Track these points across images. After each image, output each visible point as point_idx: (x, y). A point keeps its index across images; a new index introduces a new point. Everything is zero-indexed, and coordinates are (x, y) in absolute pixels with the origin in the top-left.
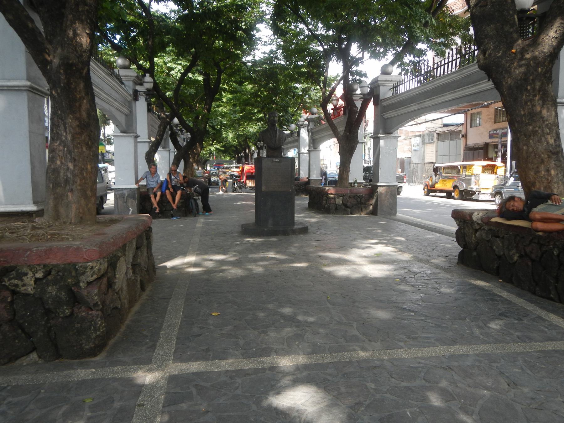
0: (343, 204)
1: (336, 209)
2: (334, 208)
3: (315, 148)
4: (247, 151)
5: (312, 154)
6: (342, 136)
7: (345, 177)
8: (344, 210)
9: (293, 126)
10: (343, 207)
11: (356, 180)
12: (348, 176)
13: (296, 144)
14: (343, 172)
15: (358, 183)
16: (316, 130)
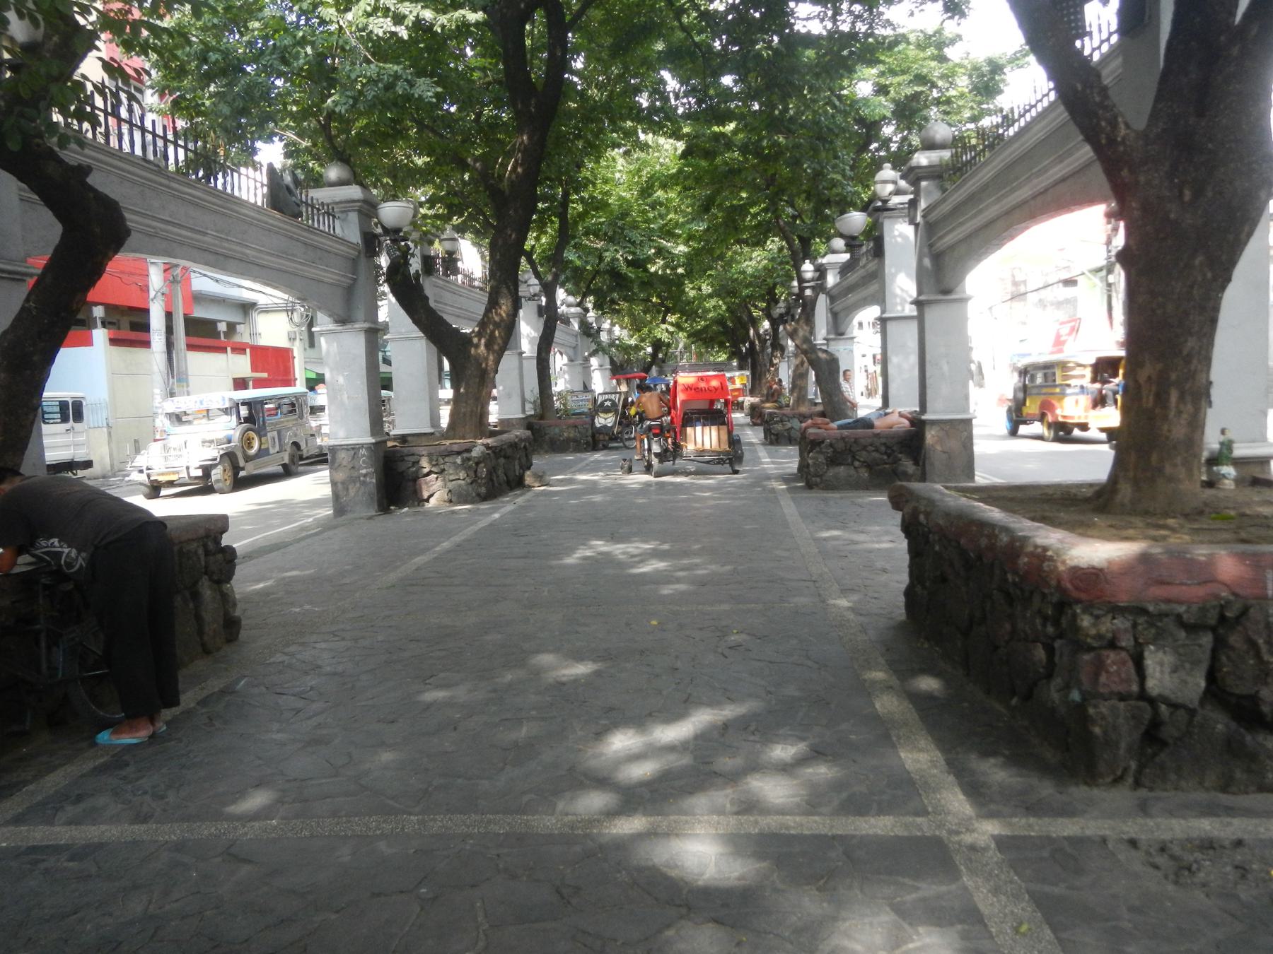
0: (1215, 690)
1: (1152, 736)
2: (1128, 735)
3: (947, 292)
4: (752, 332)
5: (932, 314)
6: (1144, 135)
7: (1179, 431)
8: (1233, 749)
9: (856, 220)
10: (1221, 723)
11: (1227, 446)
12: (1197, 425)
13: (873, 287)
14: (1161, 398)
15: (1239, 463)
16: (946, 208)
